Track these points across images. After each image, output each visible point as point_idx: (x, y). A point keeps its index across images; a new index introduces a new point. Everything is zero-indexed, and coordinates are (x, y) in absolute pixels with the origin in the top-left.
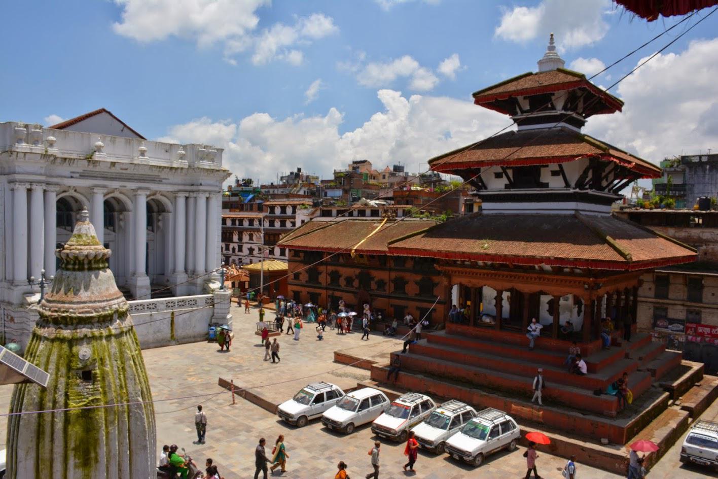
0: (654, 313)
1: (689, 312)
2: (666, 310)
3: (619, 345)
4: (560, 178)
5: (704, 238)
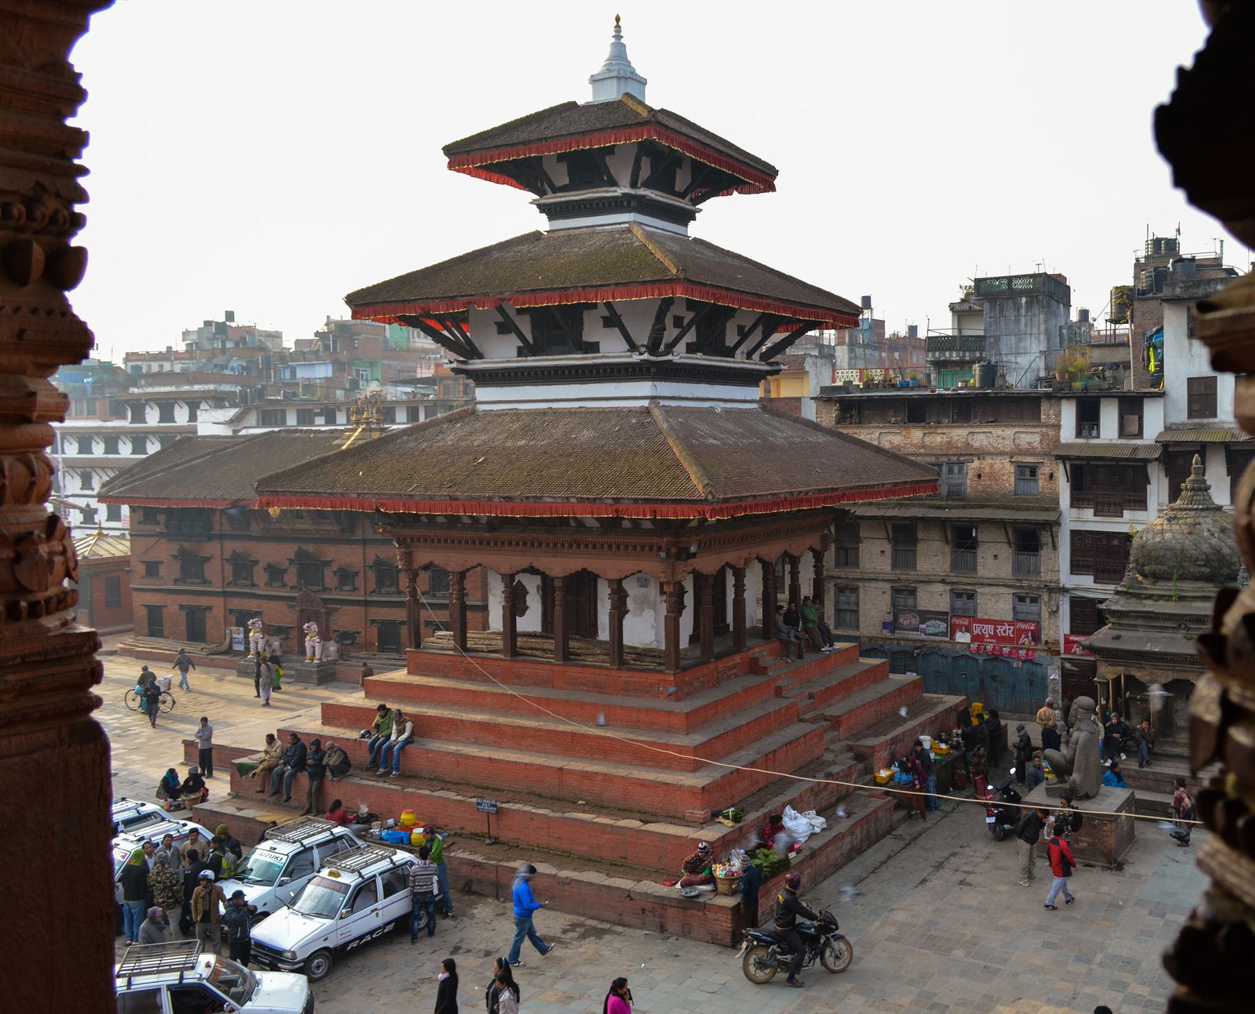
0: (894, 605)
1: (957, 595)
2: (913, 592)
3: (762, 671)
4: (617, 329)
5: (976, 444)
